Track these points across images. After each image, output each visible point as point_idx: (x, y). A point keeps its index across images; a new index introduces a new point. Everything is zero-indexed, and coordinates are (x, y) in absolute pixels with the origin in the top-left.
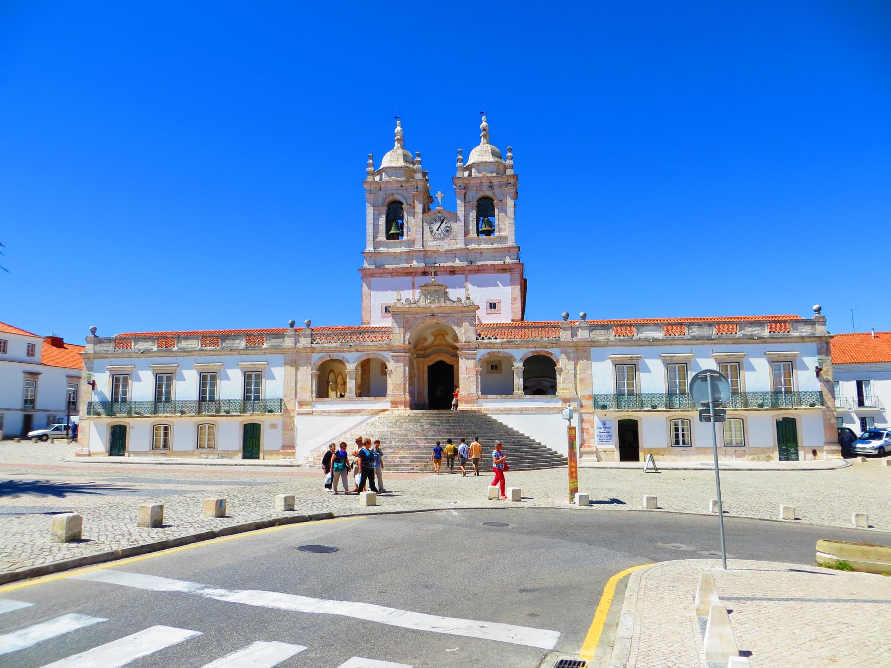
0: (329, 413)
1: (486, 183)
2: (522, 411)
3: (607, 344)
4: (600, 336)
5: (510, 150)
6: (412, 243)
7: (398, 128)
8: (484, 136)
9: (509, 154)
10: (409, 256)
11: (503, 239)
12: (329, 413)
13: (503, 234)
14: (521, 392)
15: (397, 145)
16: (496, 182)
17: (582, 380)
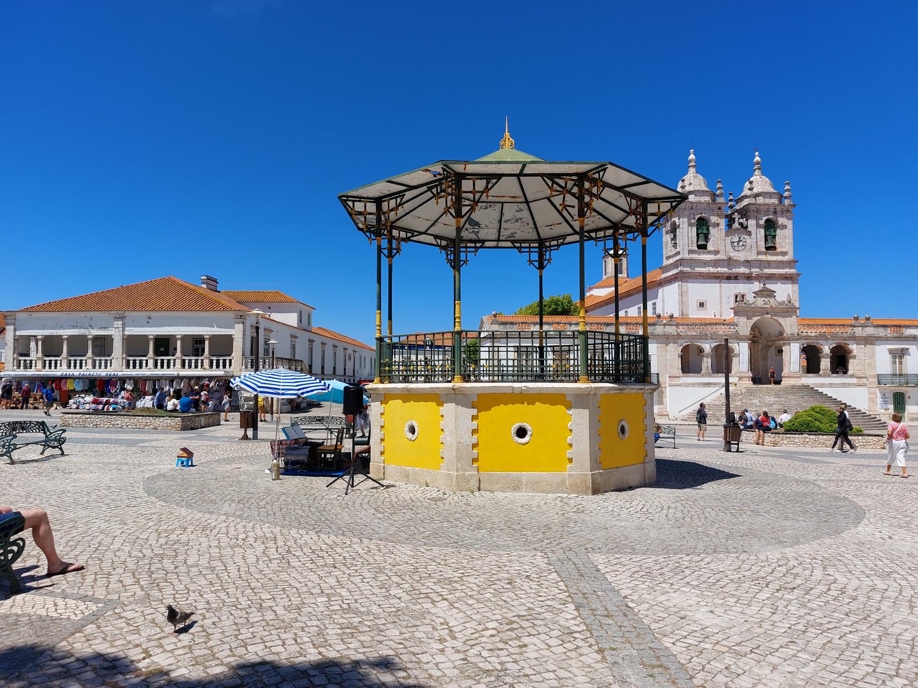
0: (694, 385)
1: (771, 209)
2: (830, 385)
3: (886, 340)
4: (881, 332)
5: (788, 184)
6: (716, 252)
7: (692, 157)
8: (759, 169)
9: (787, 187)
10: (716, 263)
11: (784, 254)
12: (694, 385)
13: (784, 250)
14: (829, 372)
15: (692, 171)
16: (778, 209)
17: (869, 364)
